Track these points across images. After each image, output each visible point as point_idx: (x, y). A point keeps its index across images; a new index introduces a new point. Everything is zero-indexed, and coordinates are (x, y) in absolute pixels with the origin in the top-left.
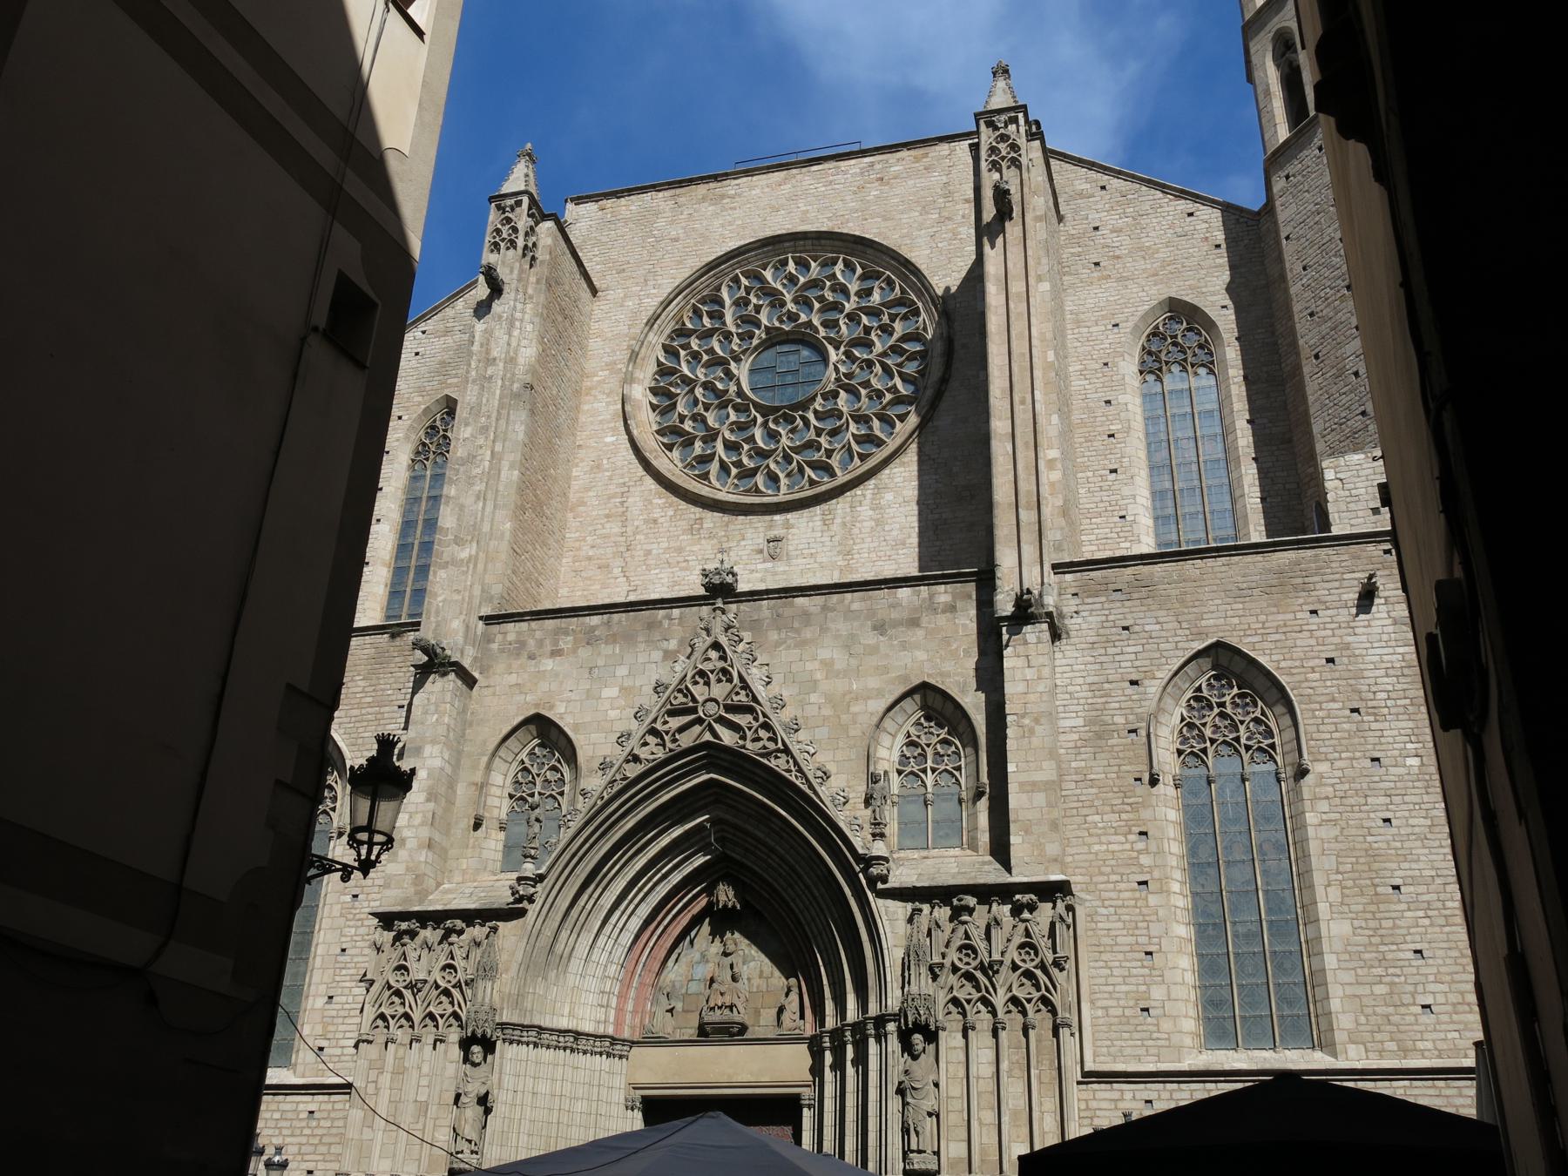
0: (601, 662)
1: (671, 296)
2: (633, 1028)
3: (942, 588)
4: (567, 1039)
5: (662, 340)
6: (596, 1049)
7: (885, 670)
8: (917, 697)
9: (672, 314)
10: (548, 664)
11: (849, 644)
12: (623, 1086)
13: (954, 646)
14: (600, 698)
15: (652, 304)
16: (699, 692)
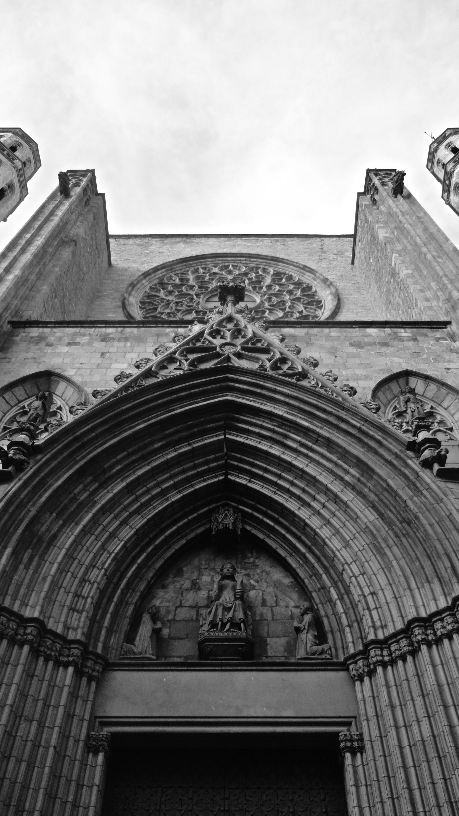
0: (112, 350)
1: (159, 267)
2: (106, 648)
3: (402, 330)
4: (28, 631)
5: (151, 285)
6: (62, 658)
7: (368, 366)
8: (402, 381)
9: (158, 276)
10: (66, 349)
11: (333, 352)
12: (87, 717)
13: (425, 356)
14: (110, 368)
15: (146, 267)
16: (217, 342)
